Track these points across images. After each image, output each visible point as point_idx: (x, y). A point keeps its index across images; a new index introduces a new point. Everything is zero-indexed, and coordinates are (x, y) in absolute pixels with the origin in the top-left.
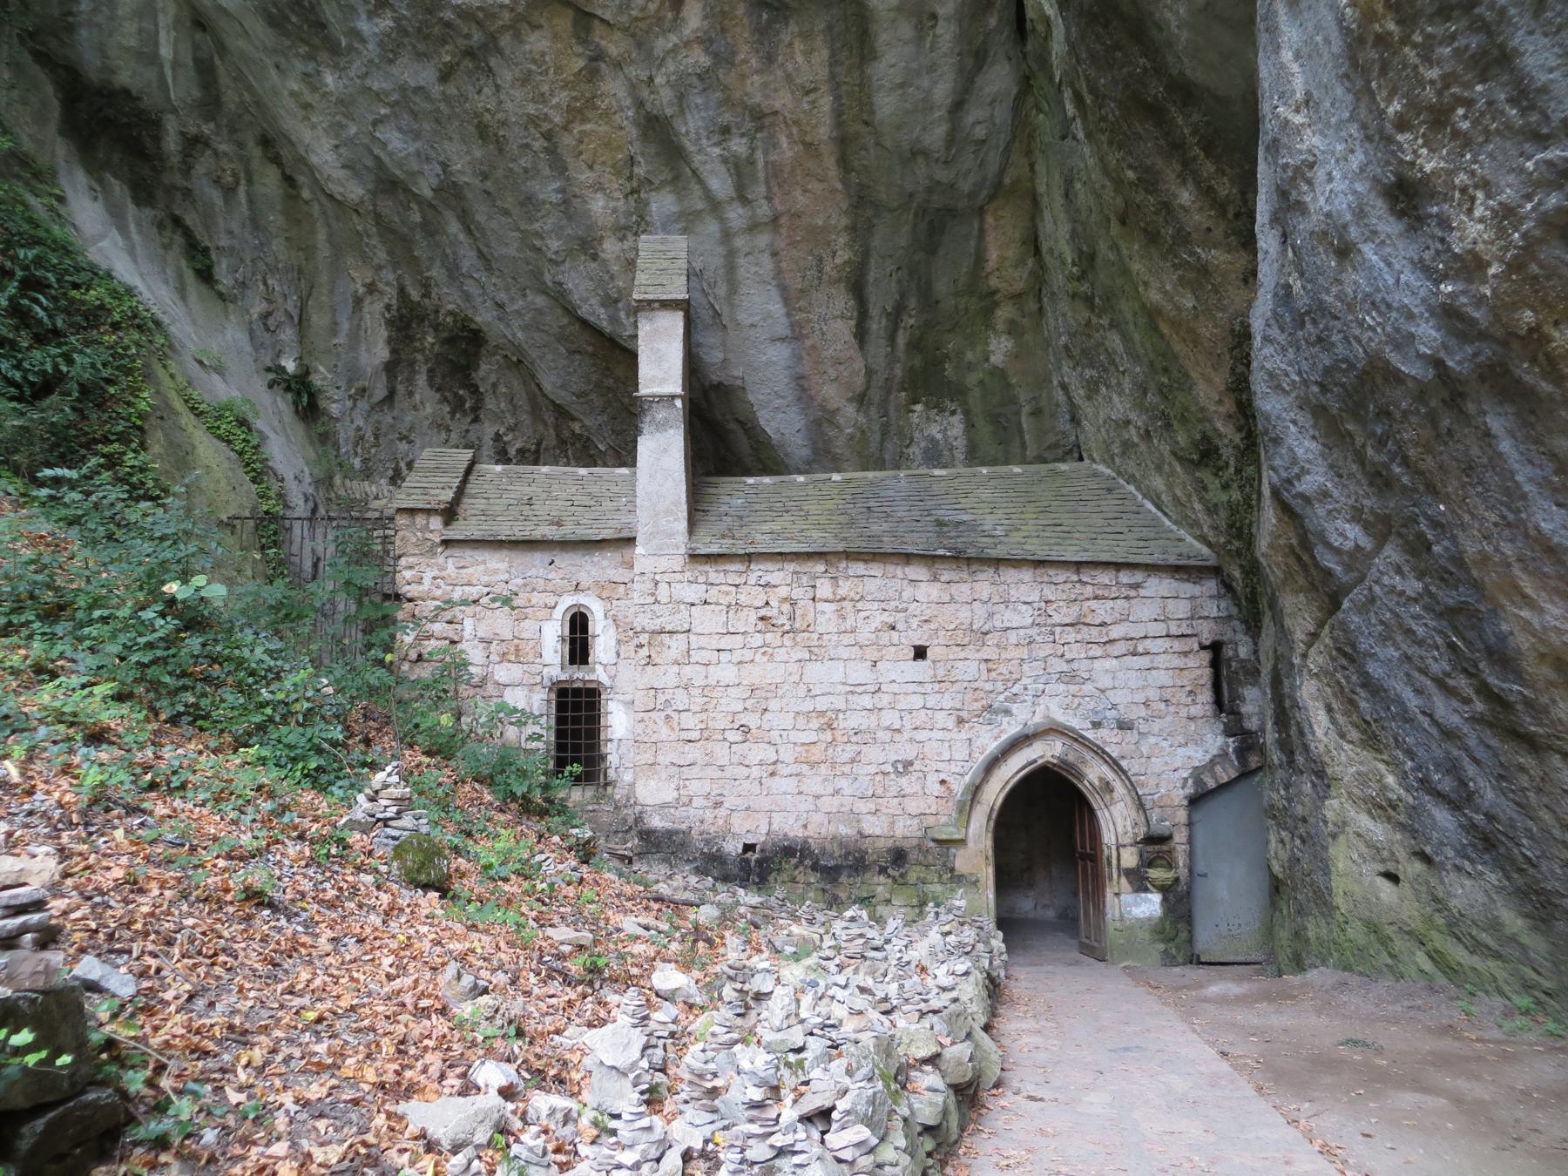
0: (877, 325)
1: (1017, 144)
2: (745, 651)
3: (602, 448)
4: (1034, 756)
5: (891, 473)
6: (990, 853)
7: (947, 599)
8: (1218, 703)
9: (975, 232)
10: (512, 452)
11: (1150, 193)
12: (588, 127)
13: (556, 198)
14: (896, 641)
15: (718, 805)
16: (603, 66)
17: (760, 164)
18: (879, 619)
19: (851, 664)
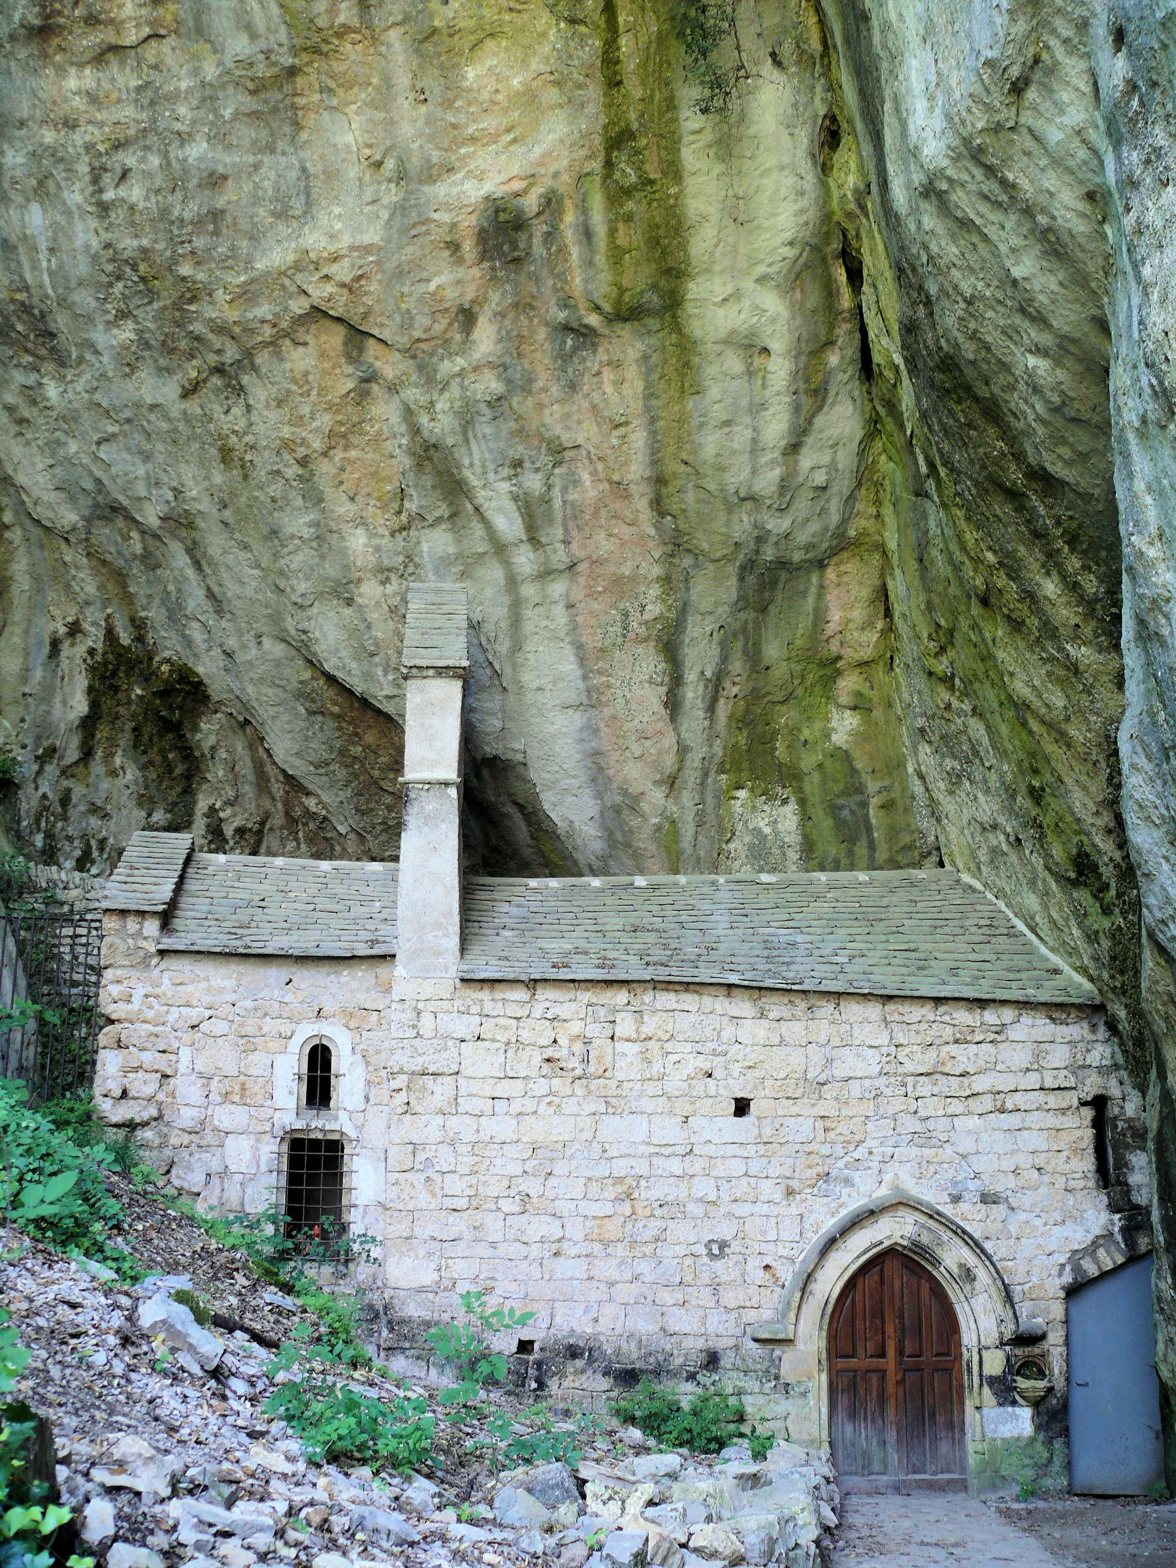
2: (526, 1101)
3: (342, 829)
4: (880, 1237)
6: (824, 1356)
7: (777, 1041)
10: (229, 831)
12: (353, 454)
14: (712, 1092)
19: (657, 1119)
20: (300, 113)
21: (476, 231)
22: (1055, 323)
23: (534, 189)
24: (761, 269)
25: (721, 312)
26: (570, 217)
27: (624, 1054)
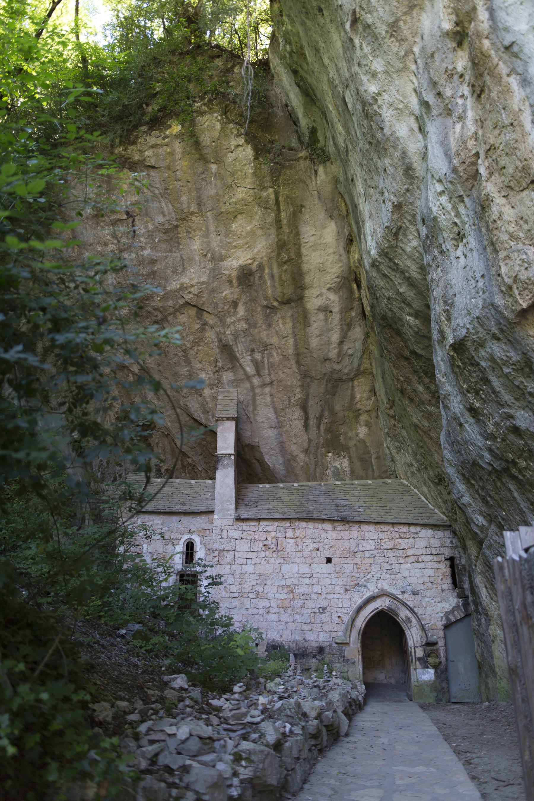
2: (257, 559)
4: (377, 606)
5: (319, 483)
6: (360, 649)
7: (340, 538)
16: (207, 327)
17: (266, 363)
18: (312, 546)
19: (301, 565)
24: (328, 286)
25: (316, 300)
26: (267, 271)
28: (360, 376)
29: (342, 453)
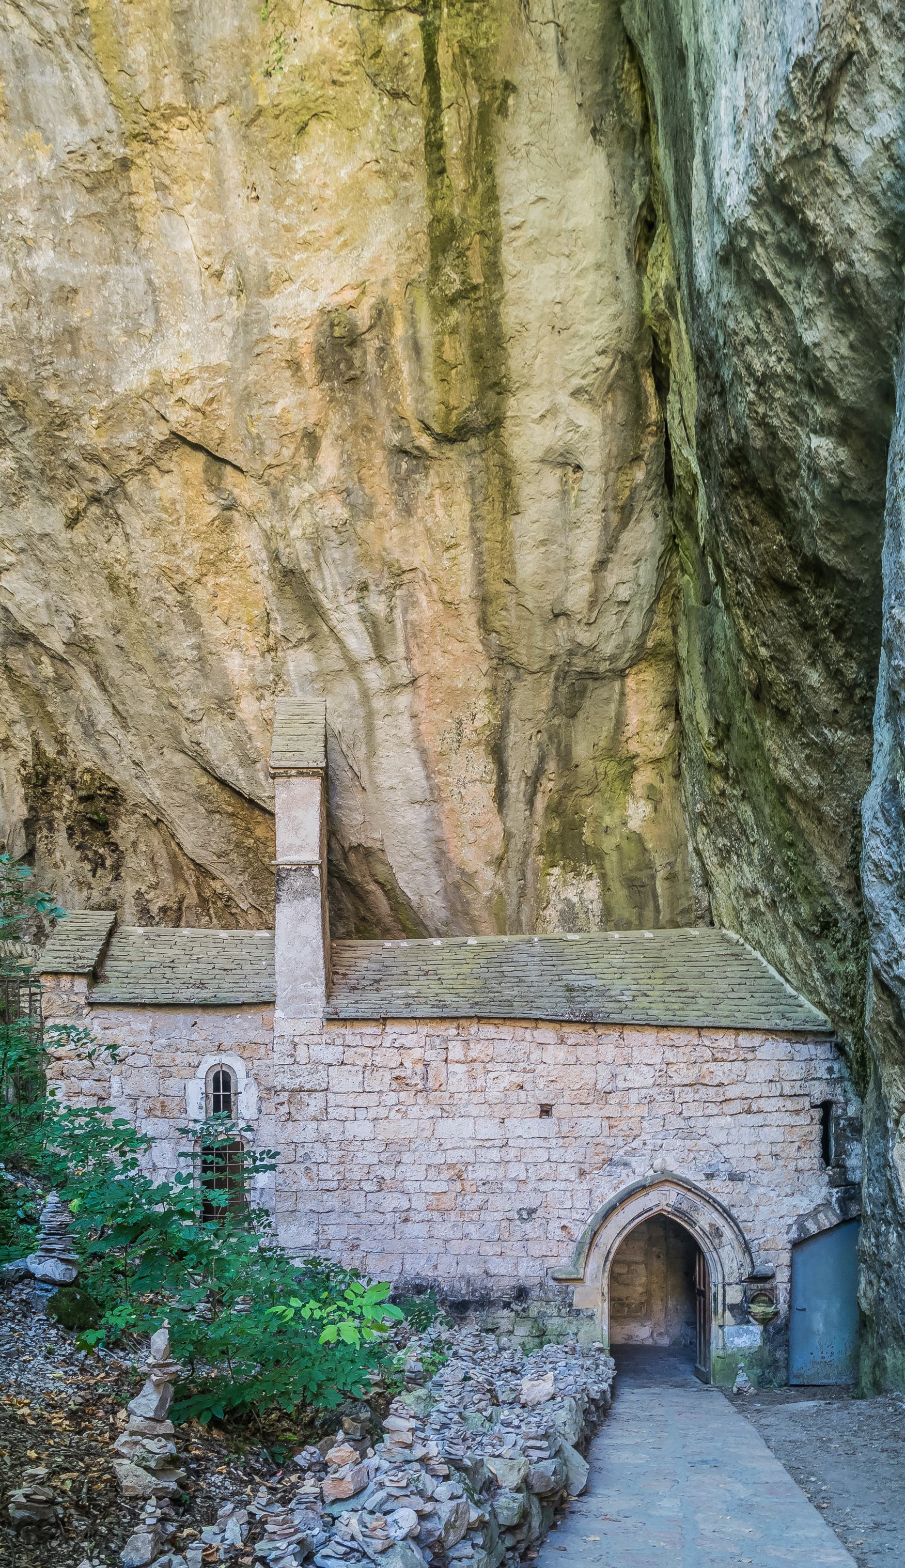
0: (516, 789)
1: (661, 606)
2: (380, 1109)
5: (527, 936)
6: (606, 1290)
7: (573, 1060)
8: (826, 1156)
9: (616, 697)
11: (782, 671)
12: (222, 580)
13: (191, 654)
14: (523, 1100)
15: (354, 1247)
16: (236, 515)
17: (399, 623)
18: (510, 1079)
19: (480, 1121)
20: (138, 215)
21: (314, 347)
22: (841, 394)
23: (365, 299)
24: (576, 382)
25: (537, 428)
26: (400, 330)
27: (455, 1073)
28: (643, 665)
29: (584, 867)
